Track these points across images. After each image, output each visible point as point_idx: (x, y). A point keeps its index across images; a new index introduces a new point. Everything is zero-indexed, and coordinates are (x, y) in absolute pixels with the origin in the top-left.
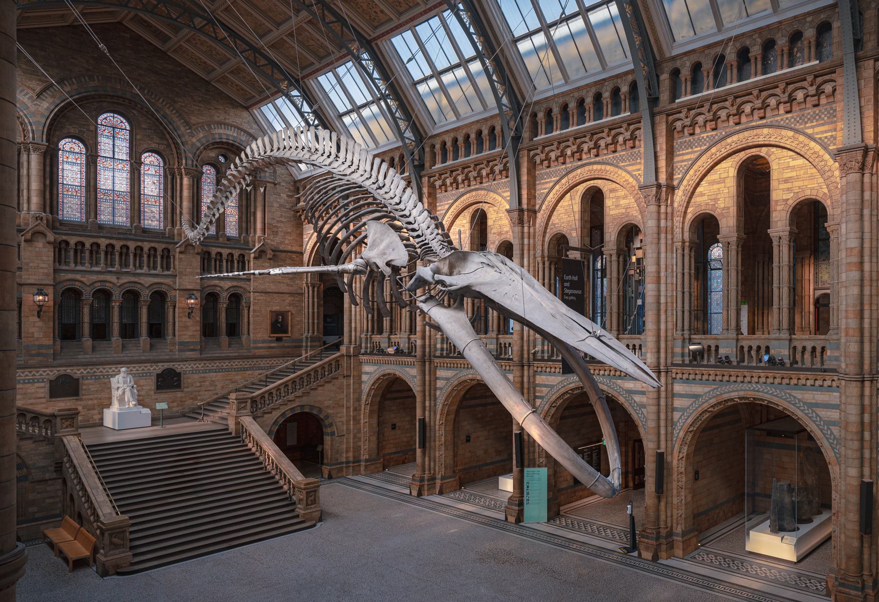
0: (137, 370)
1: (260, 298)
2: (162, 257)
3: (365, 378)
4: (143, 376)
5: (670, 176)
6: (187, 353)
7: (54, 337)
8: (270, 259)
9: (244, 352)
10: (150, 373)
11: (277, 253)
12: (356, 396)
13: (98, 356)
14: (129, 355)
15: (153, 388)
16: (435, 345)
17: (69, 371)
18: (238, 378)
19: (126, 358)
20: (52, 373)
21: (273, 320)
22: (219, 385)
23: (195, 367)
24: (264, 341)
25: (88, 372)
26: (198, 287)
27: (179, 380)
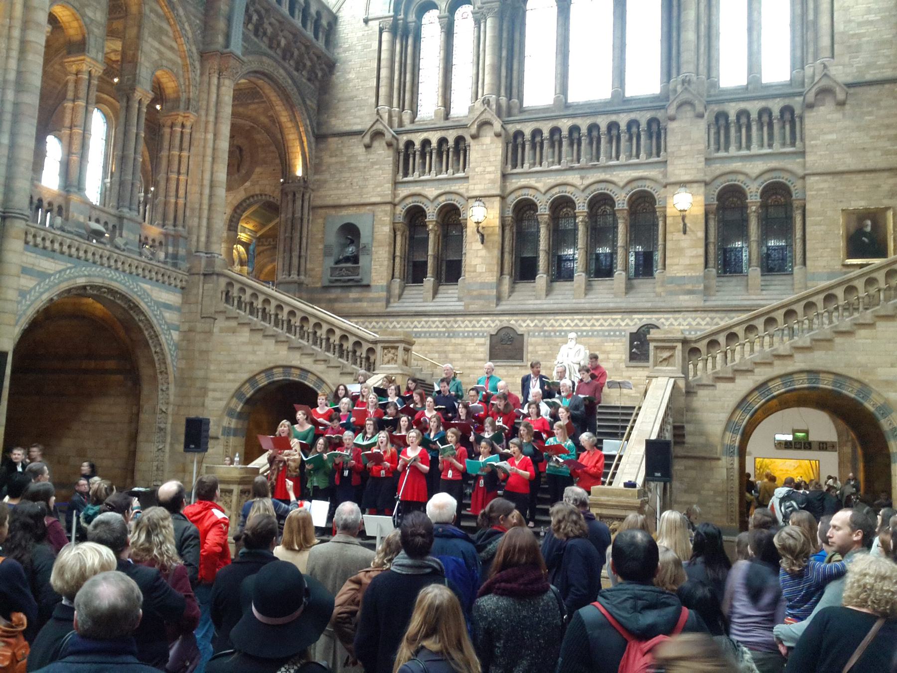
0: (601, 325)
1: (822, 186)
2: (650, 137)
4: (609, 335)
6: (681, 297)
7: (502, 273)
8: (841, 104)
10: (620, 331)
11: (858, 90)
13: (552, 302)
14: (594, 300)
15: (624, 357)
17: (512, 321)
19: (587, 306)
20: (491, 325)
21: (852, 230)
23: (694, 323)
25: (536, 326)
26: (700, 176)
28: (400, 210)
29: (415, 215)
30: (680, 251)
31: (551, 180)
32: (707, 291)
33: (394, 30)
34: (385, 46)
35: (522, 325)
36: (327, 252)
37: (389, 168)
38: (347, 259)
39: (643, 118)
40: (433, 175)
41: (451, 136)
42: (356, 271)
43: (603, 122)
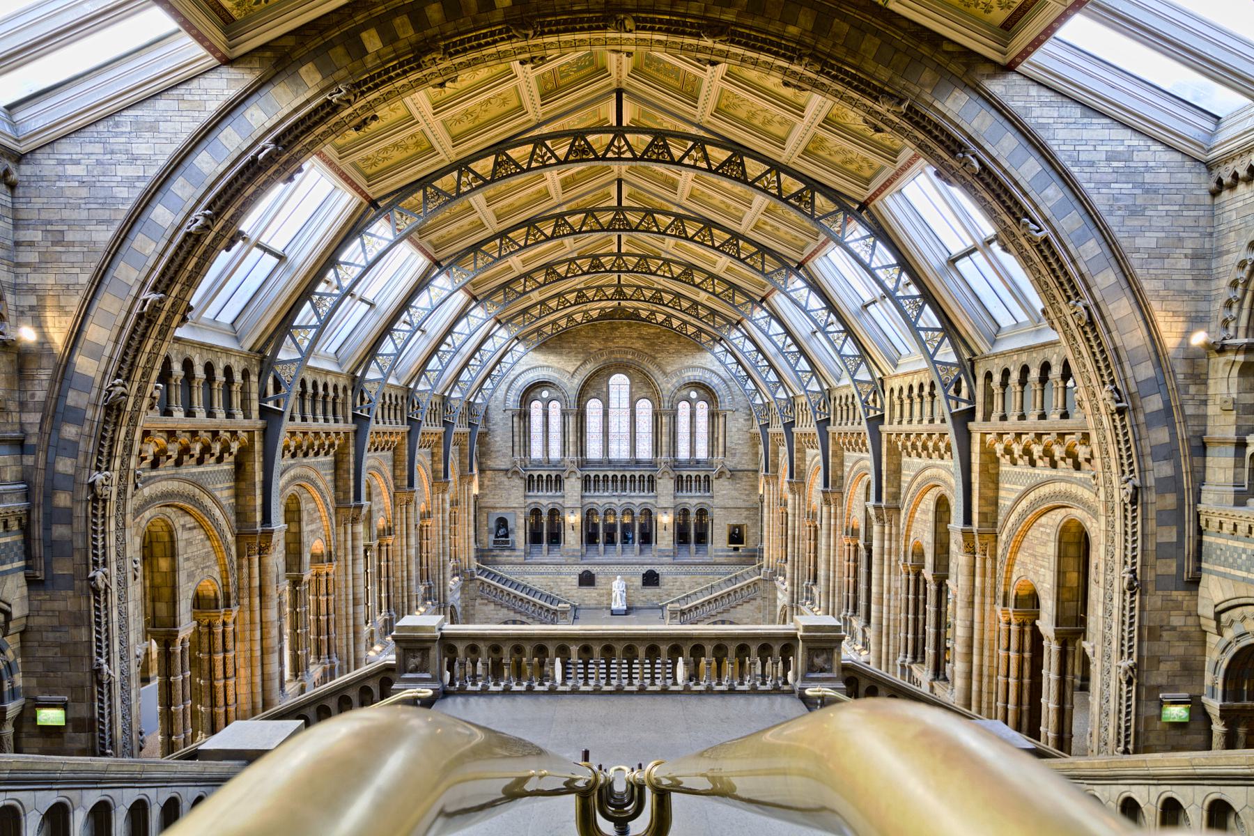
3: (778, 601)
5: (896, 496)
9: (707, 559)
12: (772, 617)
16: (802, 593)
17: (589, 568)
18: (701, 580)
20: (580, 569)
22: (687, 586)
24: (723, 551)
27: (658, 579)
28: (528, 510)
29: (536, 512)
30: (663, 538)
31: (605, 500)
32: (674, 557)
33: (520, 416)
34: (515, 425)
35: (594, 570)
36: (490, 532)
37: (522, 490)
38: (502, 536)
39: (646, 474)
40: (544, 493)
41: (554, 474)
42: (507, 542)
43: (628, 474)
